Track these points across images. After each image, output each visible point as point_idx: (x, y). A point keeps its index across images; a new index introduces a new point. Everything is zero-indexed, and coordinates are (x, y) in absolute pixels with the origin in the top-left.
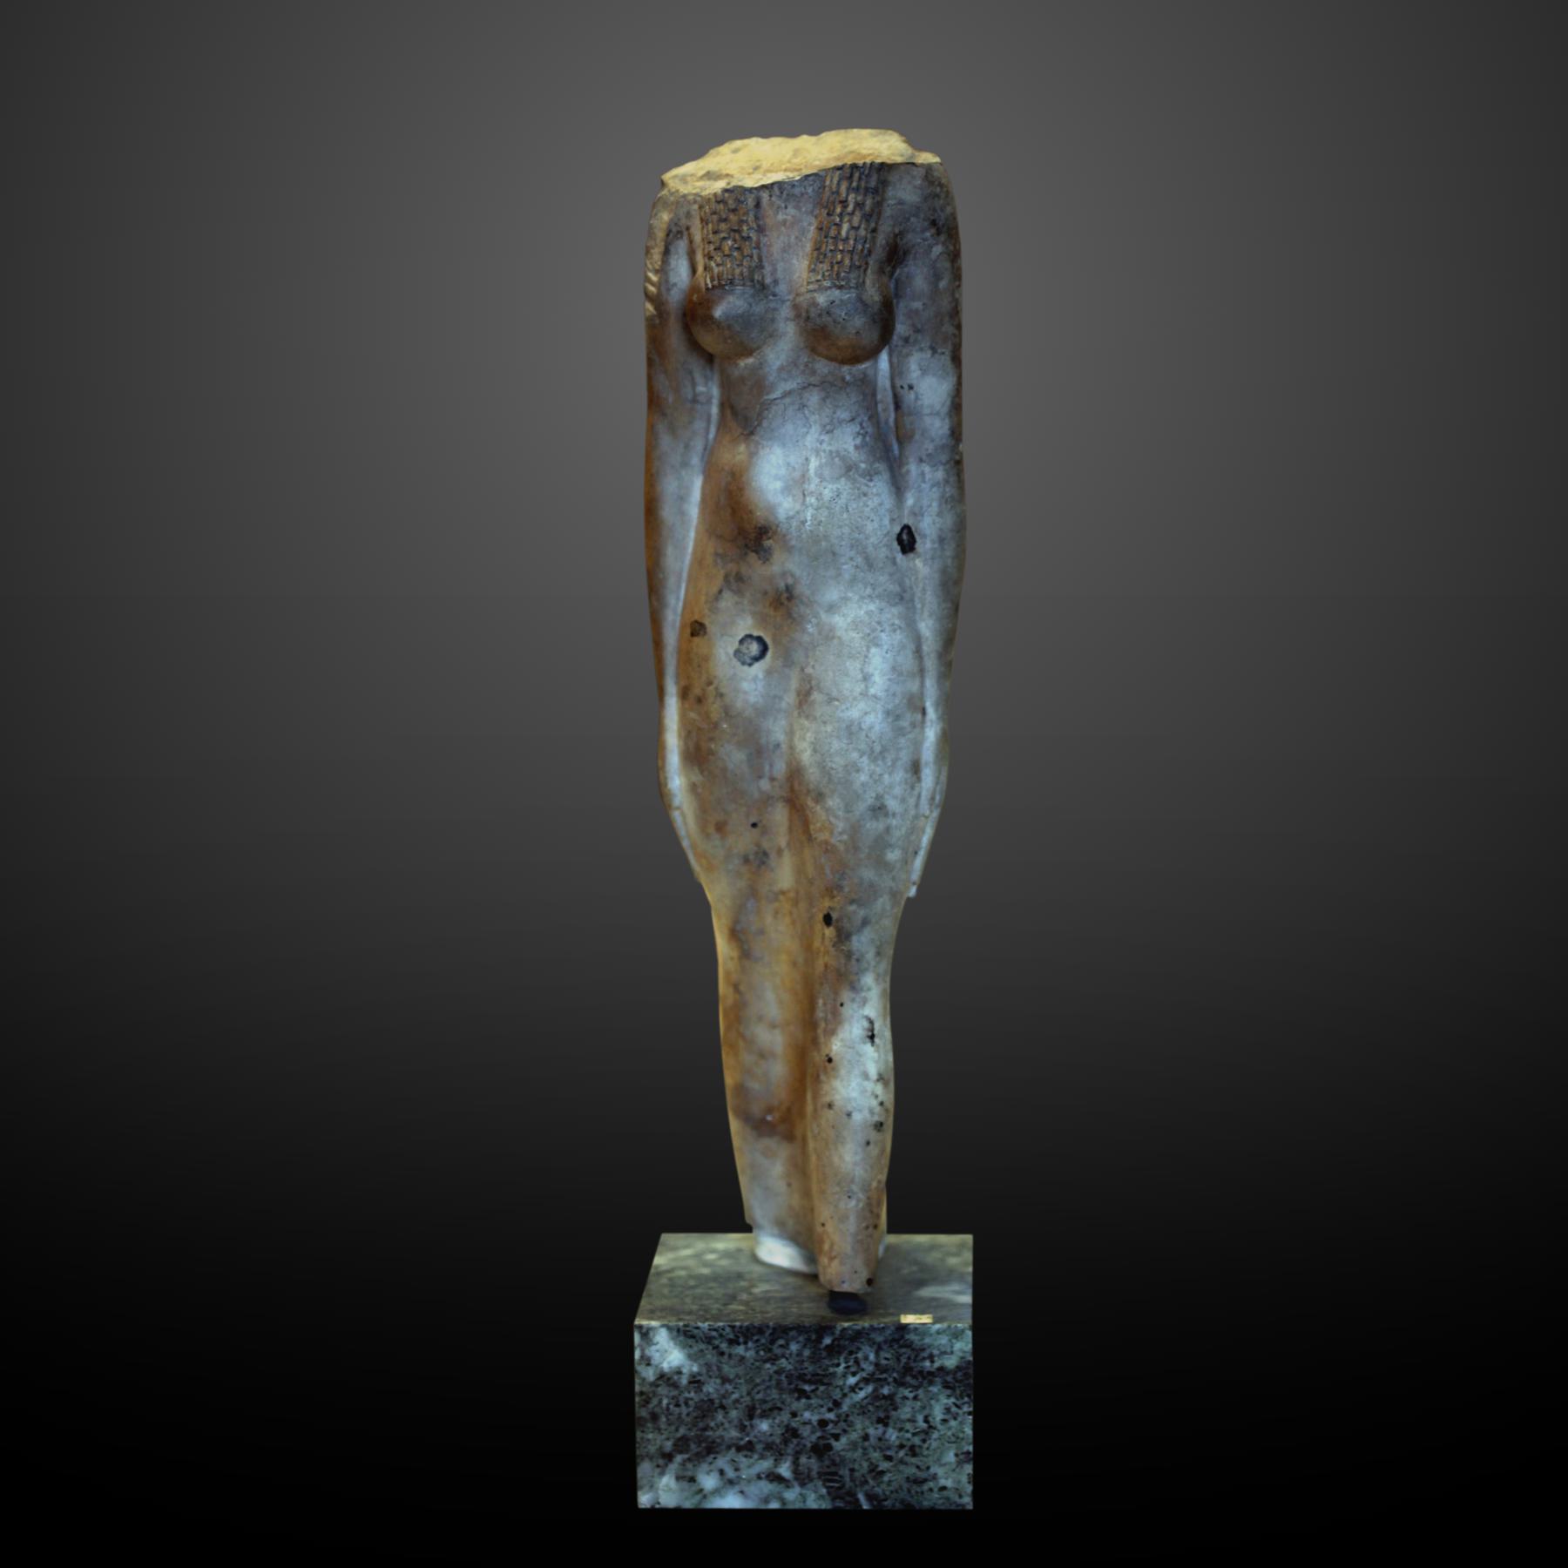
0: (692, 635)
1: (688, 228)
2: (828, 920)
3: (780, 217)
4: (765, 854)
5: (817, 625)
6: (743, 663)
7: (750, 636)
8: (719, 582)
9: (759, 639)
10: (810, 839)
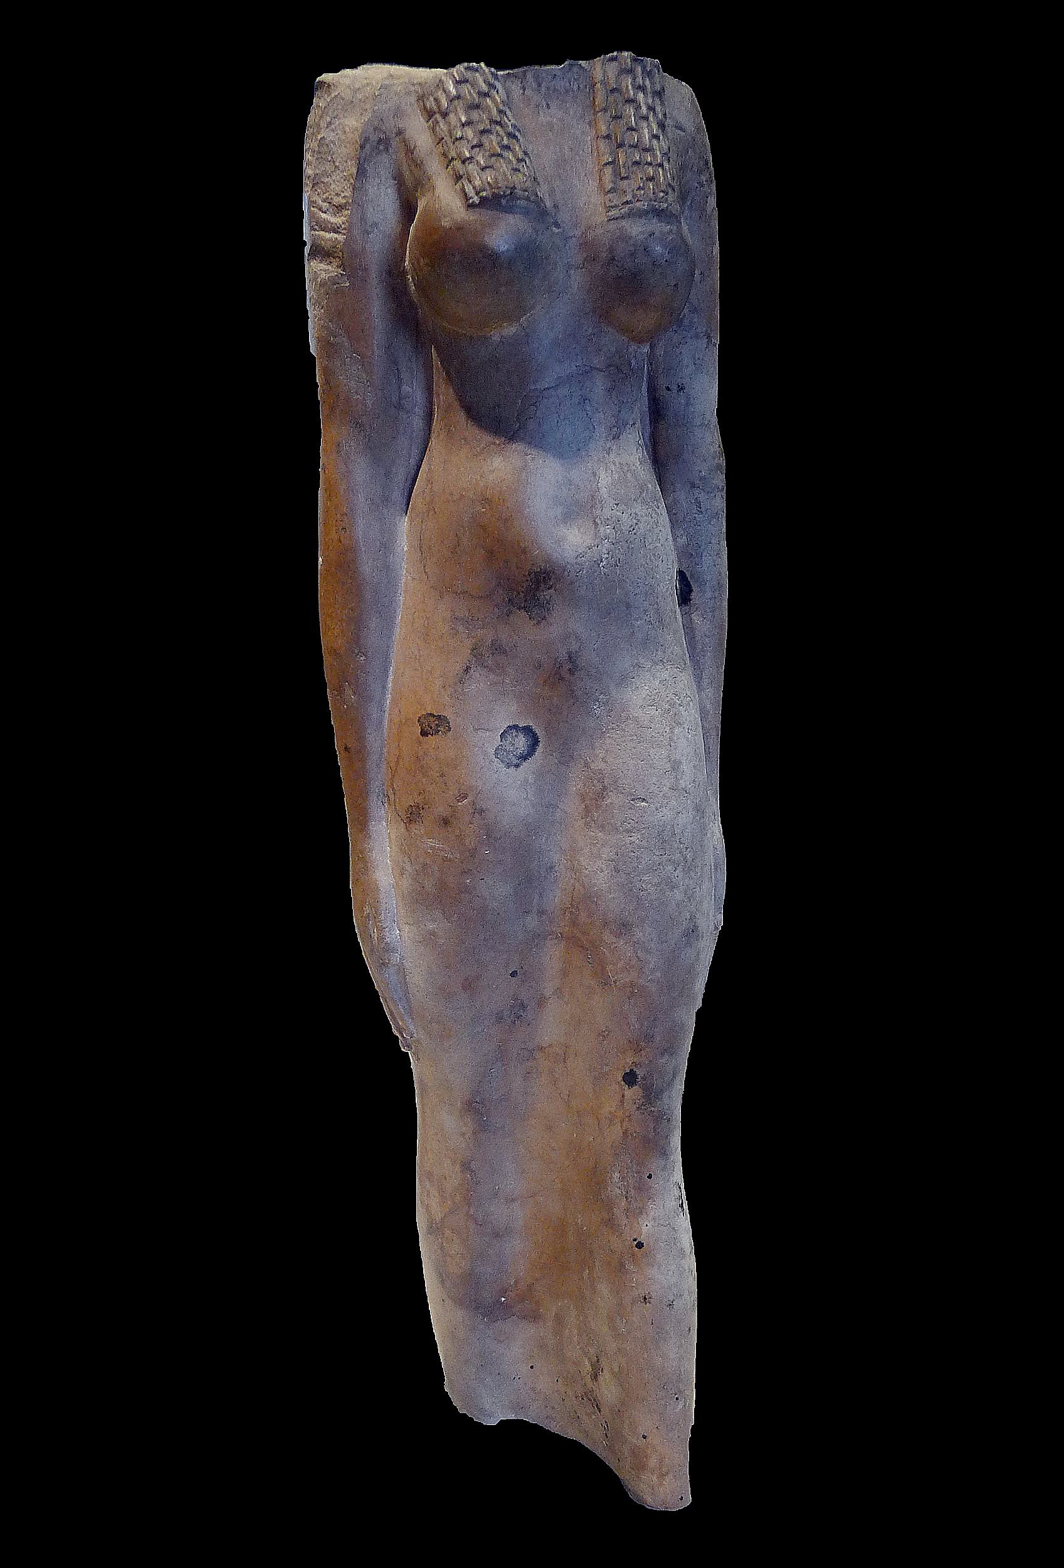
0: (424, 733)
1: (400, 133)
2: (630, 1078)
3: (542, 118)
4: (523, 1006)
5: (606, 703)
6: (508, 766)
7: (515, 727)
8: (464, 655)
9: (527, 730)
10: (606, 983)
